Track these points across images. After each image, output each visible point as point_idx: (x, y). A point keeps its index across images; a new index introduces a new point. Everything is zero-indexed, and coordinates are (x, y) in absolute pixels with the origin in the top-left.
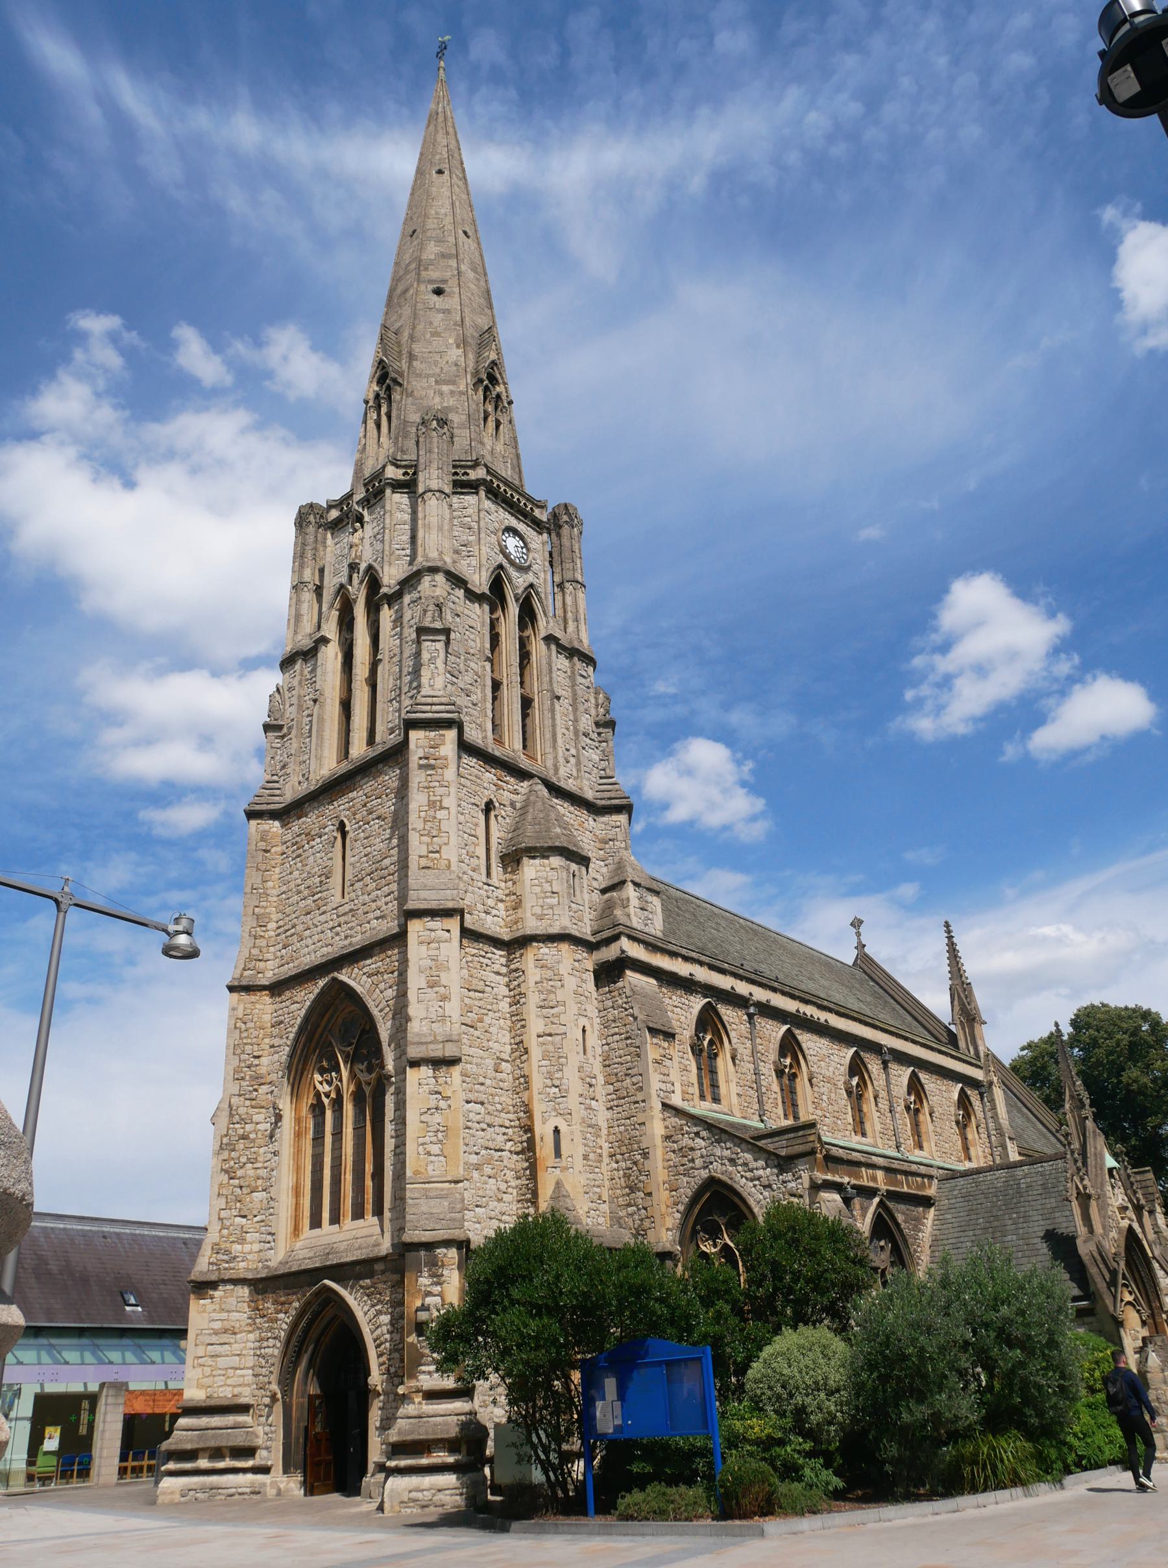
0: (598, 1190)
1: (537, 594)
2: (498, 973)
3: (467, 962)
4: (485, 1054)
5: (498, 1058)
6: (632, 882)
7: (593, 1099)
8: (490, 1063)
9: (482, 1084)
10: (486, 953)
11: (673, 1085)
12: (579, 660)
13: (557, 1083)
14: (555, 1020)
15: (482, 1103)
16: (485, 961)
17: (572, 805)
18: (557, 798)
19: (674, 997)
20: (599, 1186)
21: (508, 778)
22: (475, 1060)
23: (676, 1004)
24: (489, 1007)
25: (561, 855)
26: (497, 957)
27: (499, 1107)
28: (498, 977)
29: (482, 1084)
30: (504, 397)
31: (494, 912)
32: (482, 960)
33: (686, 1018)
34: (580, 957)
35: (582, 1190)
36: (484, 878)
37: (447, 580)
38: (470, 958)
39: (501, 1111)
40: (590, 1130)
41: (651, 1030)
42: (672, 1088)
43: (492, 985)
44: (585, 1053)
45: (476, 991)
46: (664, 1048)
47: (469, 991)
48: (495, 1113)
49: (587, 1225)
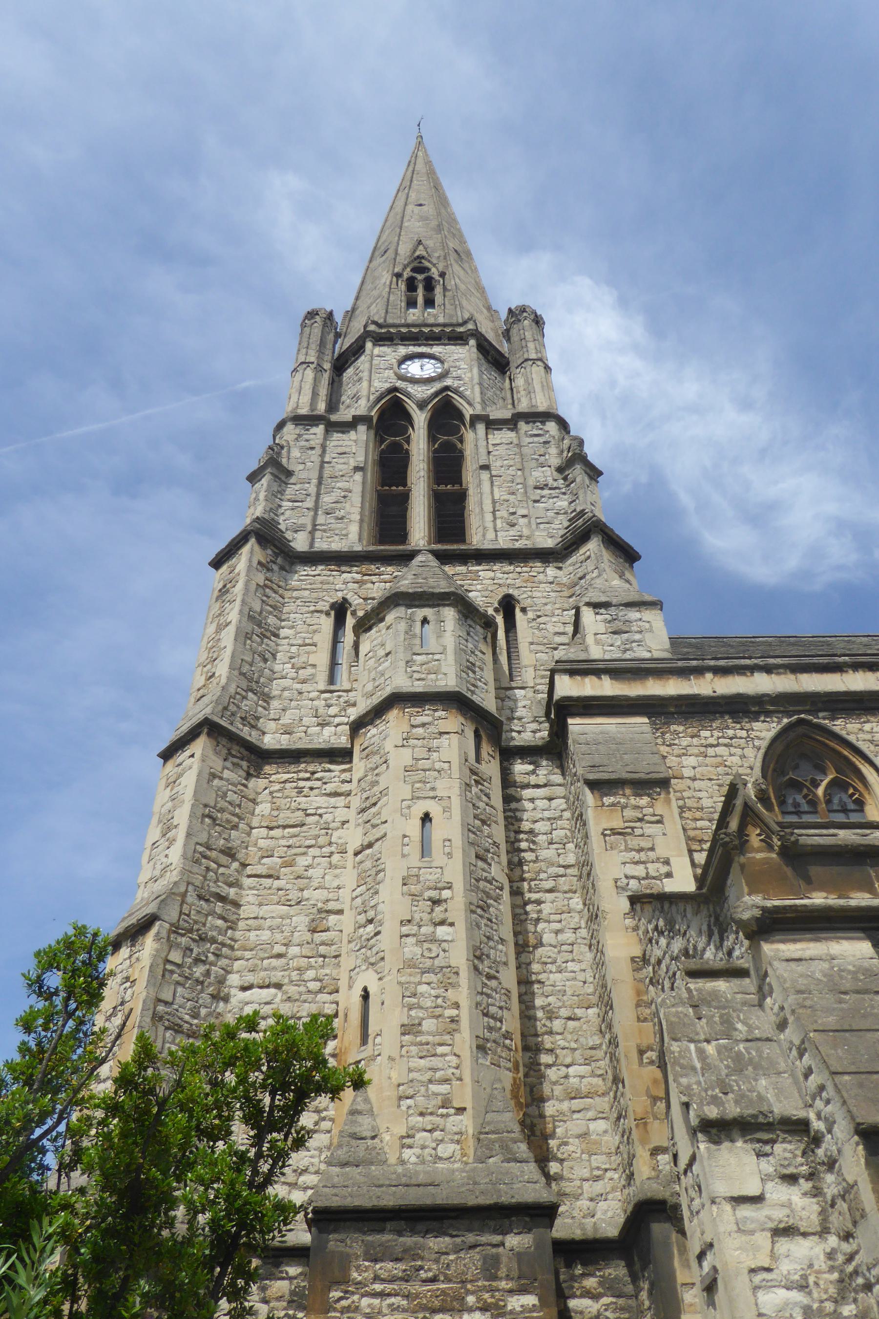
0: (444, 1089)
1: (456, 391)
2: (336, 794)
3: (271, 793)
4: (292, 911)
5: (320, 911)
6: (588, 604)
7: (442, 923)
8: (301, 921)
9: (279, 956)
10: (313, 773)
11: (667, 862)
12: (527, 423)
13: (371, 914)
14: (375, 821)
15: (278, 986)
16: (308, 784)
17: (511, 564)
18: (480, 565)
19: (705, 733)
20: (446, 1081)
21: (382, 569)
22: (268, 923)
23: (712, 741)
24: (308, 843)
25: (397, 605)
26: (337, 773)
27: (314, 986)
28: (333, 800)
29: (279, 956)
30: (412, 266)
31: (337, 720)
32: (301, 784)
33: (743, 757)
34: (429, 719)
35: (393, 1094)
36: (322, 686)
37: (296, 425)
38: (277, 787)
39: (320, 991)
40: (427, 977)
41: (594, 785)
42: (664, 869)
43: (320, 811)
44: (425, 850)
45: (285, 827)
46: (636, 807)
47: (271, 829)
48: (304, 997)
49: (402, 1162)
